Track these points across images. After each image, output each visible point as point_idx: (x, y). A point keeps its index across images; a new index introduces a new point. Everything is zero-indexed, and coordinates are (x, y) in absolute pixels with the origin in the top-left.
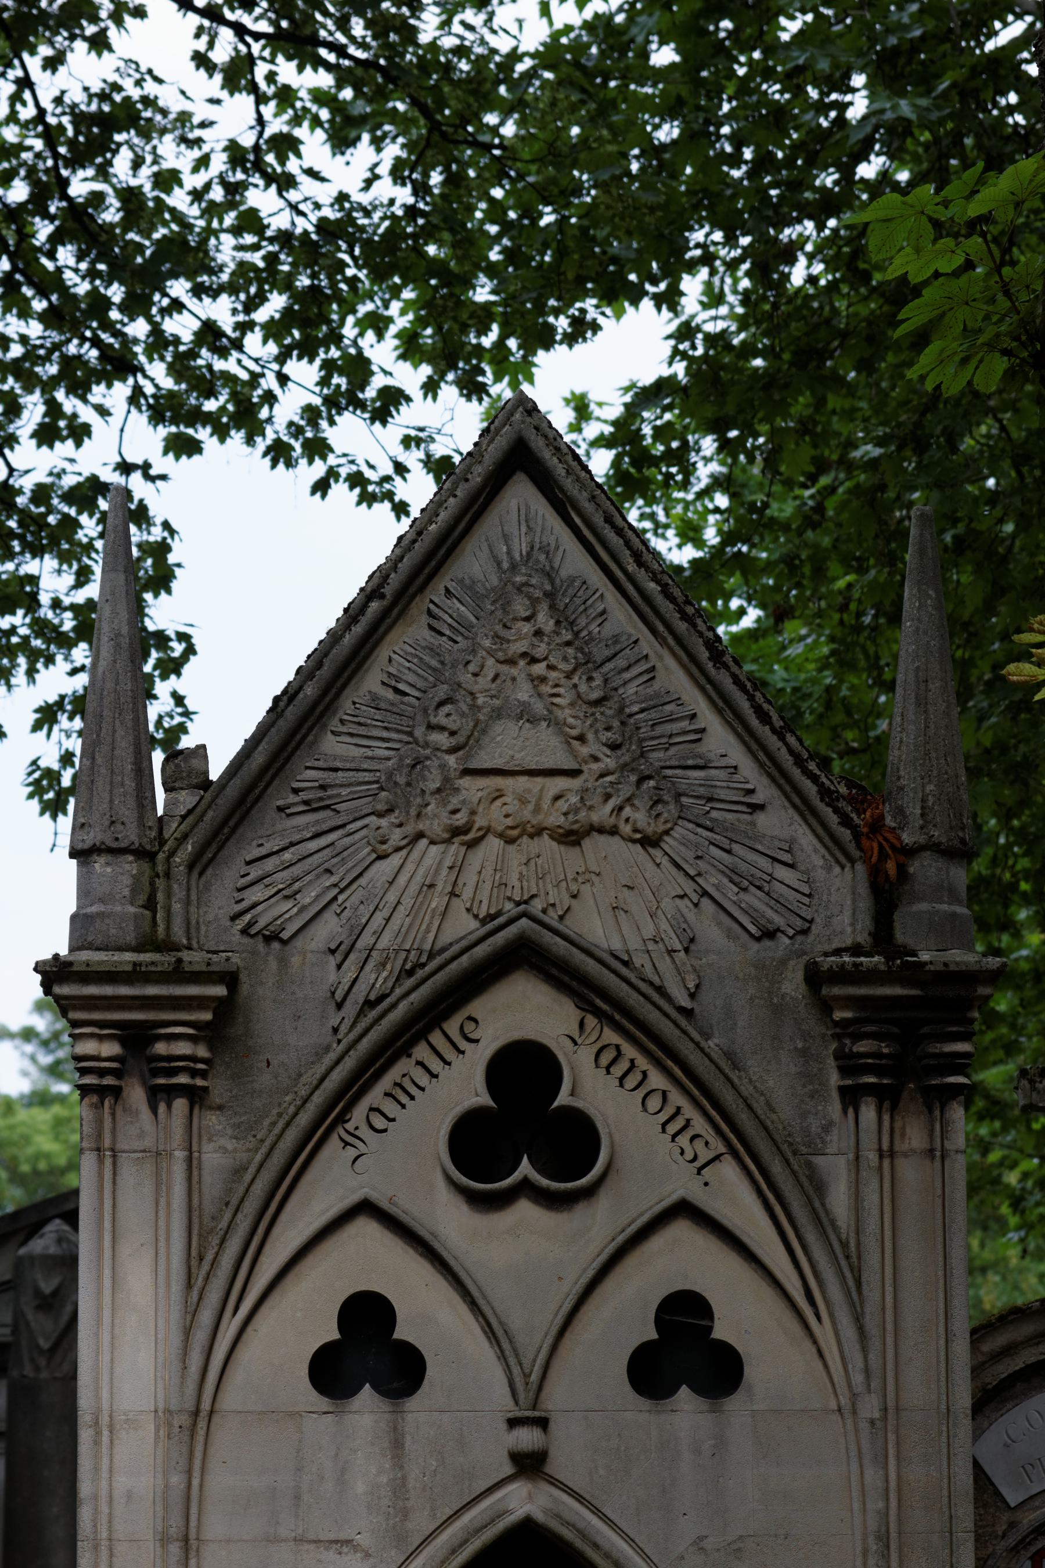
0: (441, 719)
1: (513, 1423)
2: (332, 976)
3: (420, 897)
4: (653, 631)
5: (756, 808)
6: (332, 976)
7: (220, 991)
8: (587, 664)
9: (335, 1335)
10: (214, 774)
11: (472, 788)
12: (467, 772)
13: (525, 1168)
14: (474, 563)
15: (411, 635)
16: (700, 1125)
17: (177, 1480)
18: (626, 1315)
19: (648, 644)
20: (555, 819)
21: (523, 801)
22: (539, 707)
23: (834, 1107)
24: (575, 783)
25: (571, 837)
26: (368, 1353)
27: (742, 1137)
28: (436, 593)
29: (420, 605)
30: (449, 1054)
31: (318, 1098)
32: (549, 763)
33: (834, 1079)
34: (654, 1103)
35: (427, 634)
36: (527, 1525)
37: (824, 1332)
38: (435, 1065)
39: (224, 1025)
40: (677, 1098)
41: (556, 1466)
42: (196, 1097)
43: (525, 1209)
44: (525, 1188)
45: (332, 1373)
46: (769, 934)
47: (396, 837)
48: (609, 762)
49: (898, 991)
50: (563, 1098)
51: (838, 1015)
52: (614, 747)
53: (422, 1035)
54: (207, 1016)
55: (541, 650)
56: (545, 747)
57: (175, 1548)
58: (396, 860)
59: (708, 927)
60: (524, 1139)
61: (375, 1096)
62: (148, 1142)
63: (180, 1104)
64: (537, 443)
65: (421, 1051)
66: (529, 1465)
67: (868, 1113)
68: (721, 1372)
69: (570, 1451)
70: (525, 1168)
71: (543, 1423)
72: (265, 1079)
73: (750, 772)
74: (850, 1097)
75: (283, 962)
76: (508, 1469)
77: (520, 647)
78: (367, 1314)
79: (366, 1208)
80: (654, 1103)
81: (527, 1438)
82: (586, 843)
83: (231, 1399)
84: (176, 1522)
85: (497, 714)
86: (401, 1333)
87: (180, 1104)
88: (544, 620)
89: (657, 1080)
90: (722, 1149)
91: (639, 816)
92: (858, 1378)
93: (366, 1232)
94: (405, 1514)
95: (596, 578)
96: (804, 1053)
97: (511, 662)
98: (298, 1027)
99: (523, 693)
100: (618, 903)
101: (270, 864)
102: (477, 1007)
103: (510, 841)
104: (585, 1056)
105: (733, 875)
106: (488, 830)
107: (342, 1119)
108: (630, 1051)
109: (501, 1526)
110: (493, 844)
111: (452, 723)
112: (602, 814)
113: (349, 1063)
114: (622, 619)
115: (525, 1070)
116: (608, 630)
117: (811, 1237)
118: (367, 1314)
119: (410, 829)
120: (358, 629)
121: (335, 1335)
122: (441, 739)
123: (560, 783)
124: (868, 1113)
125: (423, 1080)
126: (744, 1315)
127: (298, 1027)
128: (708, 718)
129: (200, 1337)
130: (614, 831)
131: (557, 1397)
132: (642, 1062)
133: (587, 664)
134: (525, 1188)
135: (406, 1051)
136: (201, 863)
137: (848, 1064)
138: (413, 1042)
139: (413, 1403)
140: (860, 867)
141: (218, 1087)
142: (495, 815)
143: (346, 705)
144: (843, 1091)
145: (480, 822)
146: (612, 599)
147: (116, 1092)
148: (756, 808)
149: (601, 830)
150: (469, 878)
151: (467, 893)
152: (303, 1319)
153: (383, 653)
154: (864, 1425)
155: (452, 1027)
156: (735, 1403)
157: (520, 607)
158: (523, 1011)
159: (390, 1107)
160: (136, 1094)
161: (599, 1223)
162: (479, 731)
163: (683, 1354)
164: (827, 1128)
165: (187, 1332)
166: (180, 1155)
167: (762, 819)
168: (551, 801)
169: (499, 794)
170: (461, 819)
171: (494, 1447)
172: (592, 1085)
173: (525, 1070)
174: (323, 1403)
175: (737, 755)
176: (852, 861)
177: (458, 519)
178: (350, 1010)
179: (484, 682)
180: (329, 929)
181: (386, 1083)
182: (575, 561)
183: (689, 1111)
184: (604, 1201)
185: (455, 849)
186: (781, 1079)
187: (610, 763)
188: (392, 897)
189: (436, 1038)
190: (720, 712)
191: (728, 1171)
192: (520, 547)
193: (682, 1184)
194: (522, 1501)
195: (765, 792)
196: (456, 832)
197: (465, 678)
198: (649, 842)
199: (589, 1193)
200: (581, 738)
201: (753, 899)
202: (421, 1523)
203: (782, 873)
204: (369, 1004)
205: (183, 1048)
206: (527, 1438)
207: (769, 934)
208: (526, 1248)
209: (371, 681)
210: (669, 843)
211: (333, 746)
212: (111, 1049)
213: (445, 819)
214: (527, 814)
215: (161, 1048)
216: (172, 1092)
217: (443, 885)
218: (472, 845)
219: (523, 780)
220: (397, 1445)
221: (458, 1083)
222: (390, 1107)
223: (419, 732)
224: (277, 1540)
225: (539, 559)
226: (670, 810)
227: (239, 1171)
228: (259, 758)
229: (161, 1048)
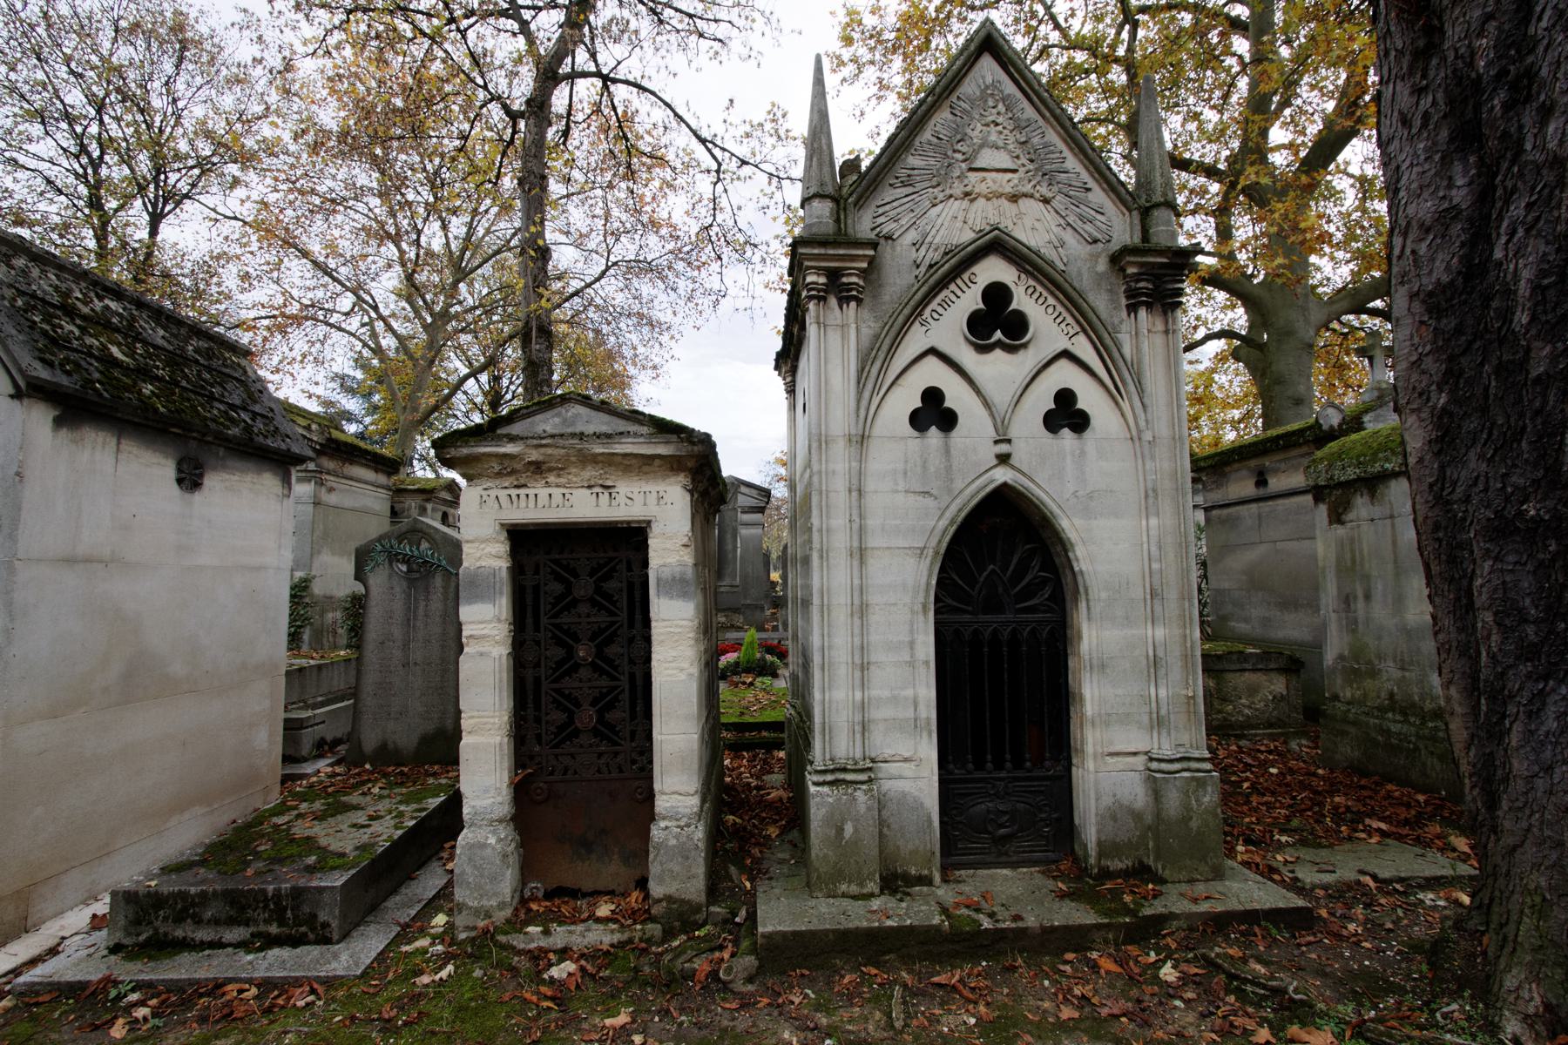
0: (958, 147)
1: (996, 442)
2: (914, 255)
3: (953, 223)
4: (1043, 117)
5: (1088, 190)
6: (914, 255)
7: (872, 253)
8: (1018, 127)
9: (919, 404)
10: (863, 168)
11: (973, 176)
12: (971, 169)
13: (998, 335)
14: (969, 87)
15: (943, 116)
16: (1070, 320)
17: (855, 464)
18: (1042, 399)
19: (1041, 122)
20: (1008, 189)
21: (994, 182)
22: (1001, 144)
23: (1124, 313)
24: (1015, 176)
25: (1014, 198)
26: (934, 413)
27: (1087, 322)
28: (954, 98)
29: (948, 103)
30: (959, 293)
31: (912, 303)
32: (1004, 166)
33: (1124, 302)
34: (1050, 310)
35: (950, 117)
36: (1005, 484)
37: (1125, 405)
38: (959, 293)
39: (871, 271)
40: (1060, 308)
41: (1014, 461)
42: (859, 301)
43: (998, 353)
44: (999, 344)
45: (918, 420)
46: (1096, 241)
47: (941, 196)
48: (1031, 167)
49: (1159, 260)
50: (1014, 306)
51: (1131, 270)
52: (1032, 161)
53: (953, 280)
54: (865, 265)
55: (1000, 120)
56: (1003, 160)
57: (855, 494)
58: (940, 207)
59: (1068, 236)
60: (997, 323)
61: (934, 305)
62: (839, 322)
63: (853, 304)
64: (996, 35)
65: (952, 287)
66: (1003, 459)
67: (1142, 313)
68: (1079, 422)
69: (1021, 453)
70: (998, 335)
71: (1009, 441)
72: (887, 298)
73: (1085, 176)
74: (1132, 309)
75: (893, 248)
76: (995, 462)
77: (991, 118)
78: (932, 396)
79: (933, 351)
80: (1050, 310)
81: (1003, 448)
82: (1020, 201)
83: (876, 431)
84: (855, 481)
85: (982, 146)
86: (948, 404)
87: (853, 304)
88: (1001, 107)
89: (1051, 301)
90: (1078, 329)
91: (1044, 190)
92: (1142, 424)
93: (932, 361)
94: (952, 480)
95: (1019, 95)
96: (1110, 291)
97: (987, 125)
98: (899, 276)
99: (993, 138)
100: (1034, 227)
101: (887, 208)
102: (976, 269)
103: (989, 199)
104: (1022, 289)
105: (1081, 217)
106: (979, 195)
107: (920, 314)
108: (1039, 288)
109: (988, 489)
110: (981, 201)
111: (964, 149)
112: (1028, 188)
113: (924, 289)
114: (1030, 112)
115: (997, 294)
116: (1025, 116)
117: (1121, 364)
118: (932, 396)
119: (948, 192)
120: (924, 108)
121: (919, 404)
122: (959, 156)
123: (1010, 175)
124: (1142, 313)
125: (954, 298)
126: (1089, 398)
127: (899, 276)
128: (1067, 153)
129: (864, 403)
130: (1032, 196)
131: (1013, 433)
132: (1045, 294)
133: (1018, 127)
134: (999, 344)
135: (946, 286)
136: (860, 203)
137: (1131, 294)
138: (949, 283)
139: (955, 433)
140: (1135, 213)
141: (867, 300)
142: (982, 188)
143: (917, 143)
144: (1128, 306)
145: (977, 190)
146: (1025, 103)
147: (824, 299)
148: (1088, 190)
149: (1025, 195)
150: (971, 216)
151: (970, 222)
152: (907, 398)
153: (932, 122)
154: (1146, 445)
155: (965, 276)
156: (1088, 434)
157: (991, 103)
158: (994, 270)
159: (940, 310)
160: (833, 301)
161: (1027, 361)
162: (976, 152)
163: (1066, 415)
164: (1121, 322)
165: (859, 401)
166: (854, 326)
167: (1090, 195)
168: (1005, 183)
169: (984, 180)
170: (968, 189)
171: (989, 452)
172: (1022, 300)
173: (997, 294)
174: (916, 434)
175: (1079, 168)
176: (1130, 211)
177: (964, 65)
178: (923, 269)
179: (976, 133)
180: (912, 236)
181: (938, 300)
182: (1010, 88)
183: (1065, 314)
184: (1031, 350)
185: (966, 203)
186: (1104, 301)
187: (1031, 167)
188: (939, 222)
189: (959, 281)
190: (1071, 149)
191: (1082, 338)
192: (989, 80)
193: (1063, 344)
194: (1002, 475)
195: (1091, 184)
196: (967, 194)
197: (969, 131)
198: (1046, 201)
199: (1025, 346)
200: (1018, 157)
201: (1088, 227)
202: (959, 484)
203: (1099, 217)
204: (931, 266)
205: (854, 279)
206: (1003, 448)
207: (1096, 241)
208: (999, 370)
209: (927, 135)
210: (1054, 203)
211: (913, 161)
212: (822, 280)
213: (962, 188)
214: (994, 188)
215: (845, 280)
216: (849, 299)
217: (961, 218)
218: (972, 201)
219: (994, 174)
220: (947, 451)
221: (968, 299)
222: (940, 310)
223: (950, 153)
224: (897, 491)
225: (995, 85)
226: (1055, 189)
227: (877, 337)
228: (883, 160)
229: (845, 280)
